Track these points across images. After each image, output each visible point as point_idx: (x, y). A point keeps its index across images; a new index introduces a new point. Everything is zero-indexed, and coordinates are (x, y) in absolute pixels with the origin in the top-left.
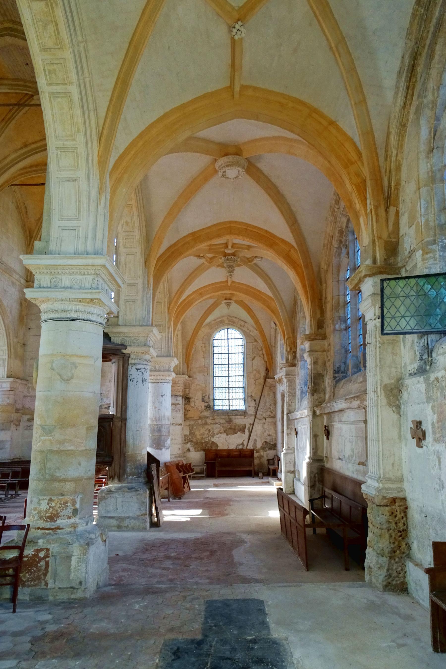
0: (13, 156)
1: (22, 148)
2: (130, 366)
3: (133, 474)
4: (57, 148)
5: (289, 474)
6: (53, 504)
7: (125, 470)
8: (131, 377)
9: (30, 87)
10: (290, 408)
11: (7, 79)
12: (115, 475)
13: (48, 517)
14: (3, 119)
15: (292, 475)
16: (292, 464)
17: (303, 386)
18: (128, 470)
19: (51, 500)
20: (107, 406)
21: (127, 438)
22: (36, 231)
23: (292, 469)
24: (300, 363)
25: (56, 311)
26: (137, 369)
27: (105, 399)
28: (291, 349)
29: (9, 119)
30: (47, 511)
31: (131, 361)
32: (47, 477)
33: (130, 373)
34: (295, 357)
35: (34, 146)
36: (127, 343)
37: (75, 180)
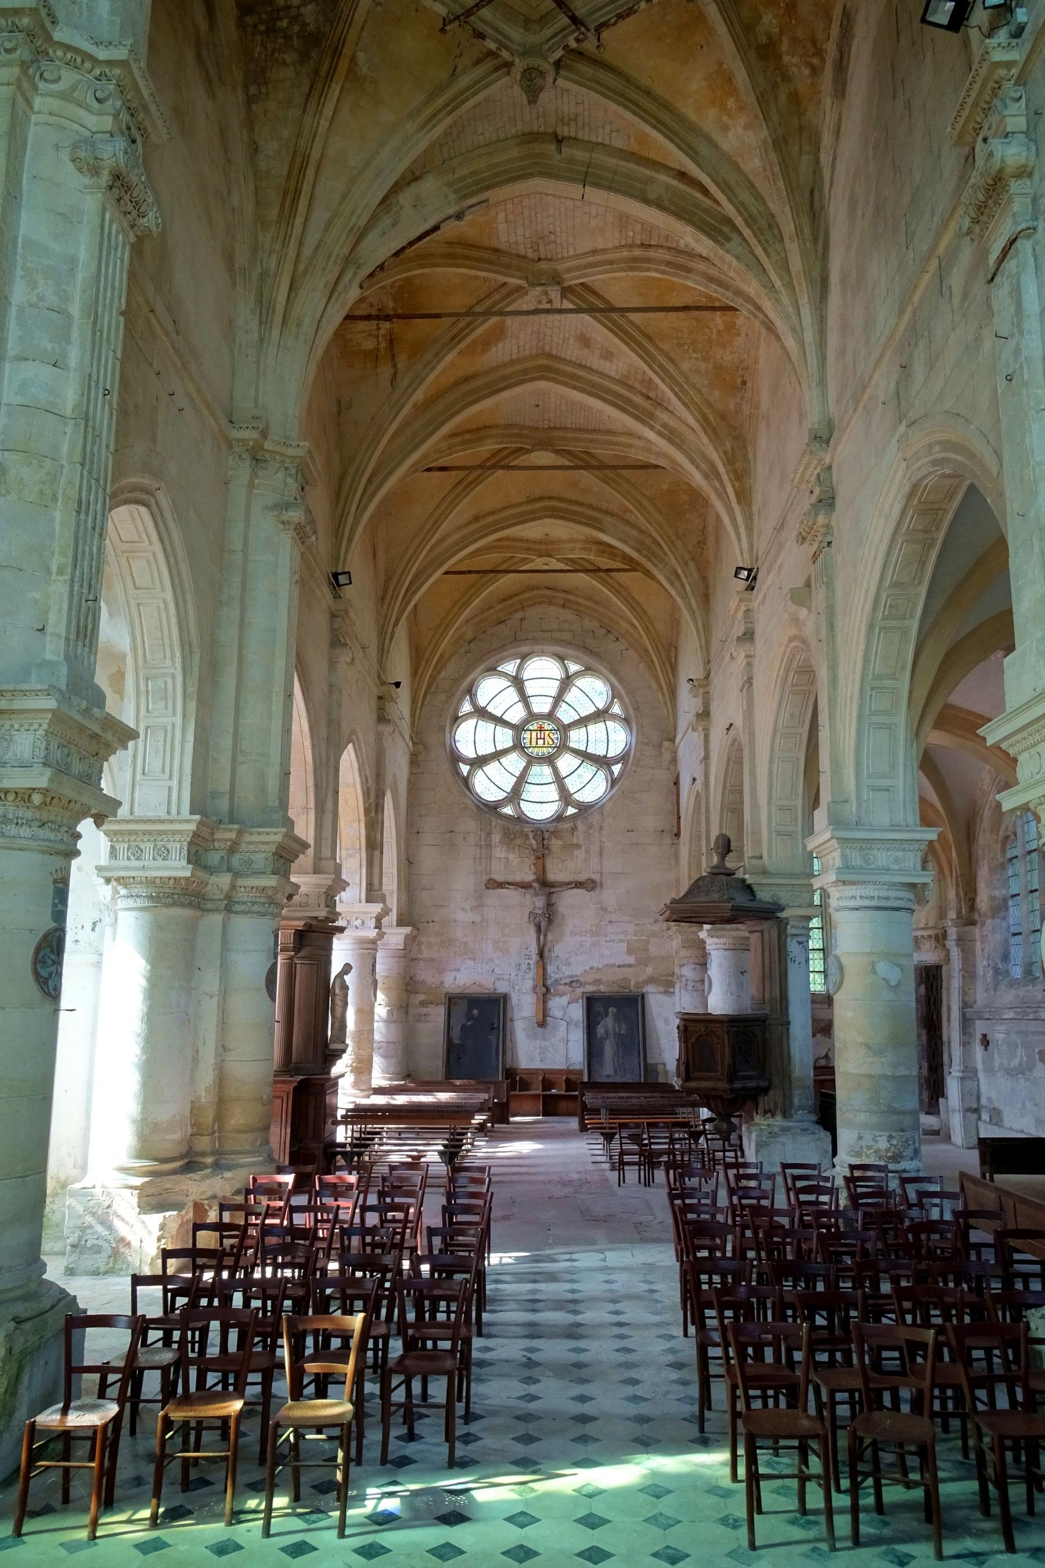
0: (456, 537)
1: (469, 523)
2: (789, 939)
3: (801, 1108)
4: (872, 689)
5: (969, 1114)
6: (895, 1142)
7: (791, 1102)
8: (791, 955)
9: (527, 436)
10: (967, 999)
11: (497, 426)
12: (776, 1108)
13: (890, 1158)
14: (459, 482)
15: (974, 1116)
16: (974, 1098)
17: (999, 962)
18: (796, 1101)
19: (890, 1137)
20: (568, 981)
21: (792, 1052)
22: (430, 648)
23: (975, 1106)
24: (989, 922)
25: (873, 898)
26: (800, 943)
27: (564, 968)
28: (966, 894)
29: (471, 482)
30: (887, 1150)
31: (790, 930)
32: (882, 1108)
33: (789, 949)
34: (972, 908)
35: (490, 519)
36: (783, 902)
37: (889, 727)
